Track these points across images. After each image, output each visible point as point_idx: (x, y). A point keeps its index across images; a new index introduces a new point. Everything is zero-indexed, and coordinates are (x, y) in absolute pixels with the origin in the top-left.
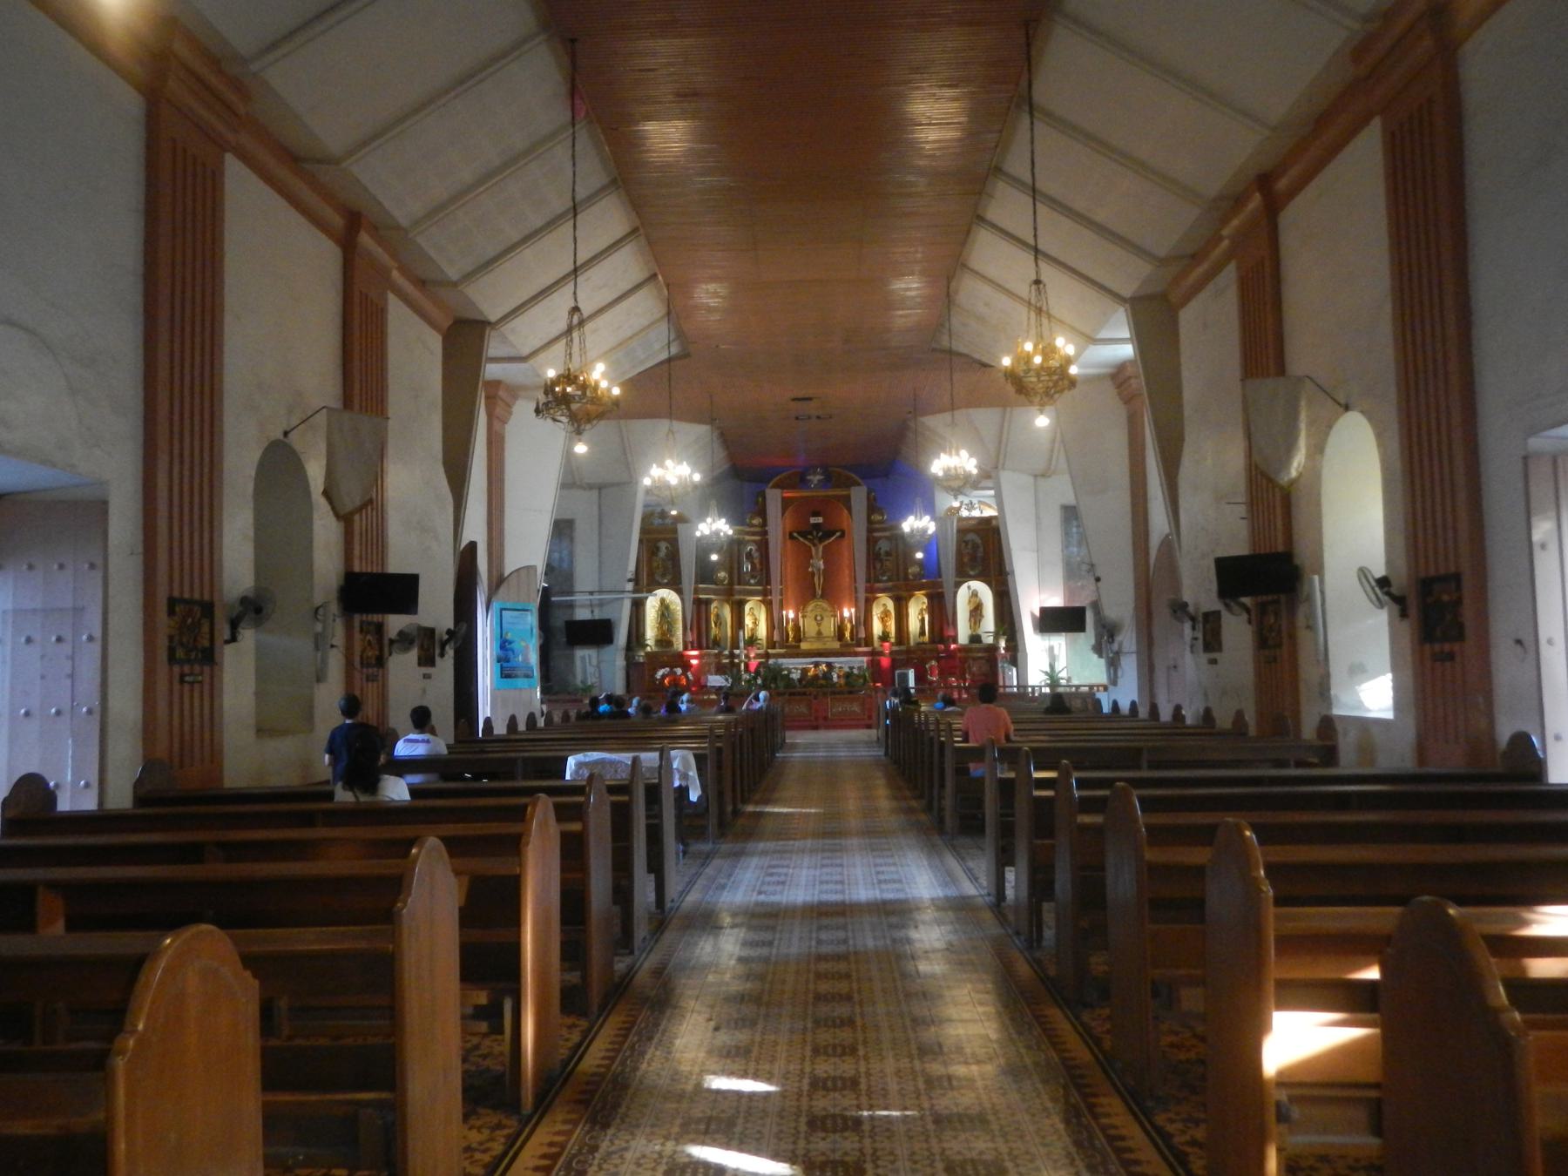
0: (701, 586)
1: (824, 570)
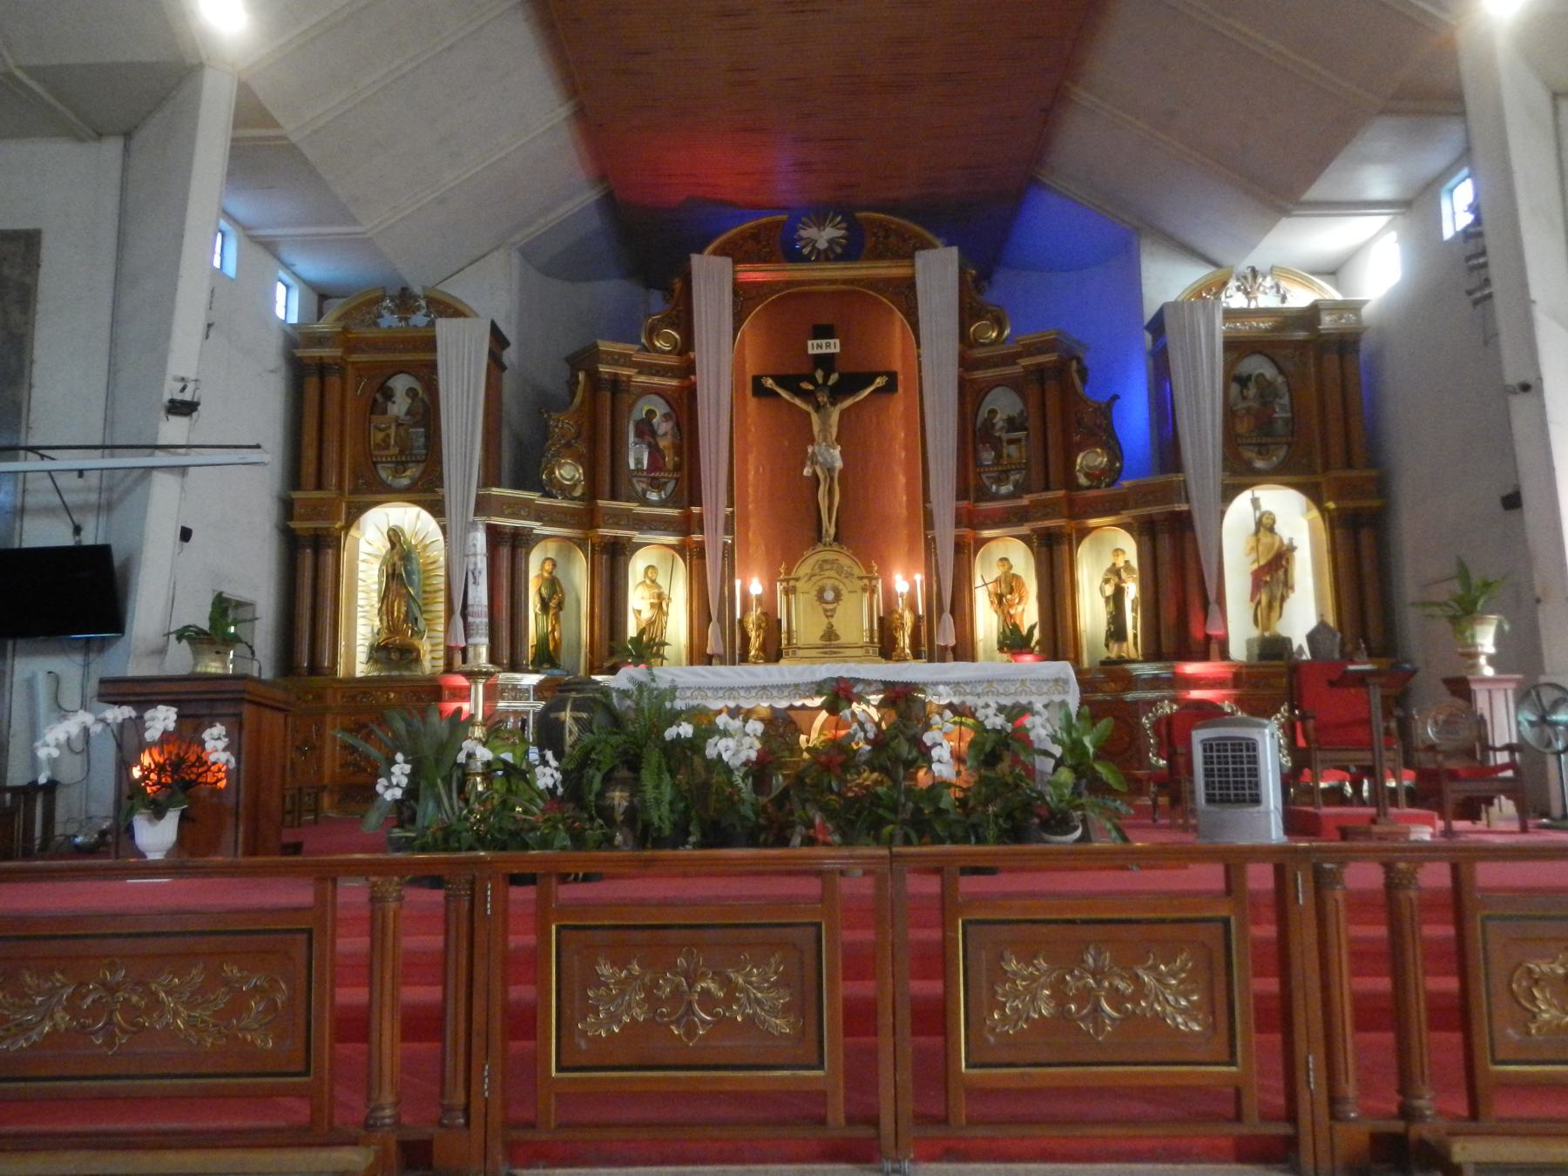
0: (495, 491)
1: (841, 471)
